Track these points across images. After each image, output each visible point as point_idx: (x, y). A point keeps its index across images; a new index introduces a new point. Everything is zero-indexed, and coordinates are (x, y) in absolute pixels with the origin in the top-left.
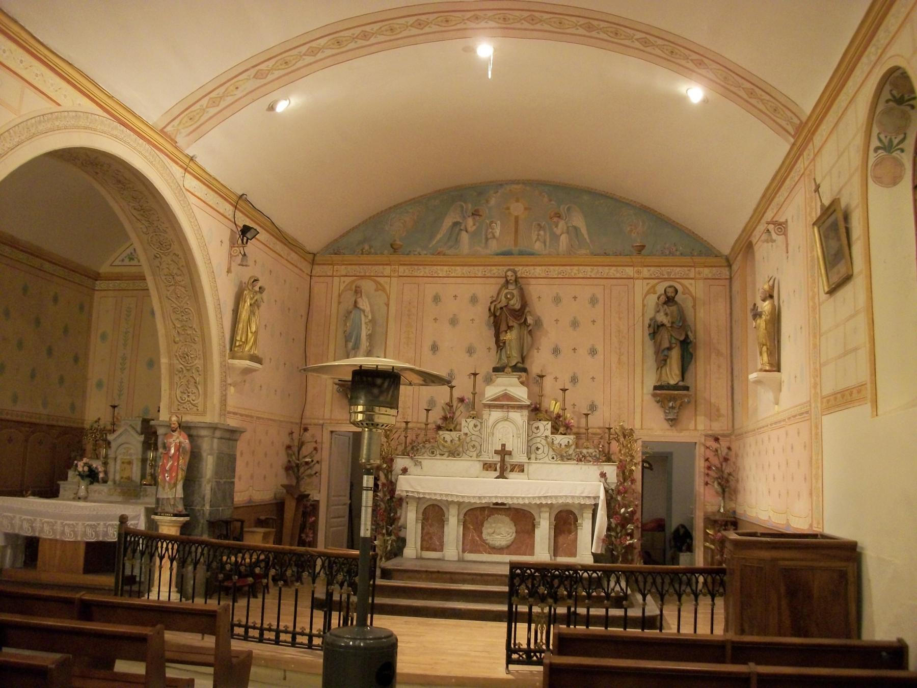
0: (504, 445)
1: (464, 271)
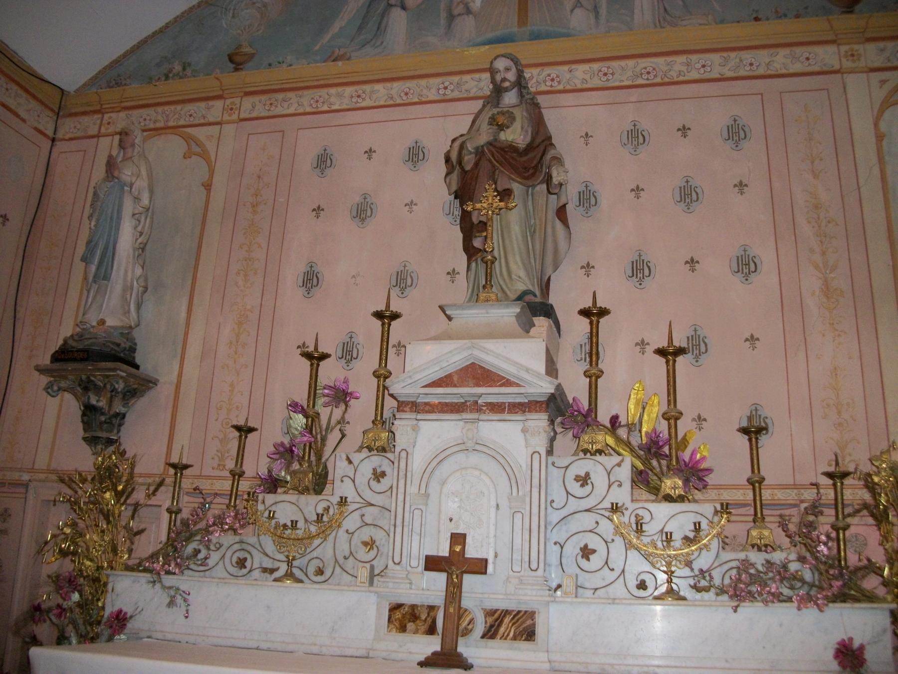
0: (458, 539)
1: (394, 92)
